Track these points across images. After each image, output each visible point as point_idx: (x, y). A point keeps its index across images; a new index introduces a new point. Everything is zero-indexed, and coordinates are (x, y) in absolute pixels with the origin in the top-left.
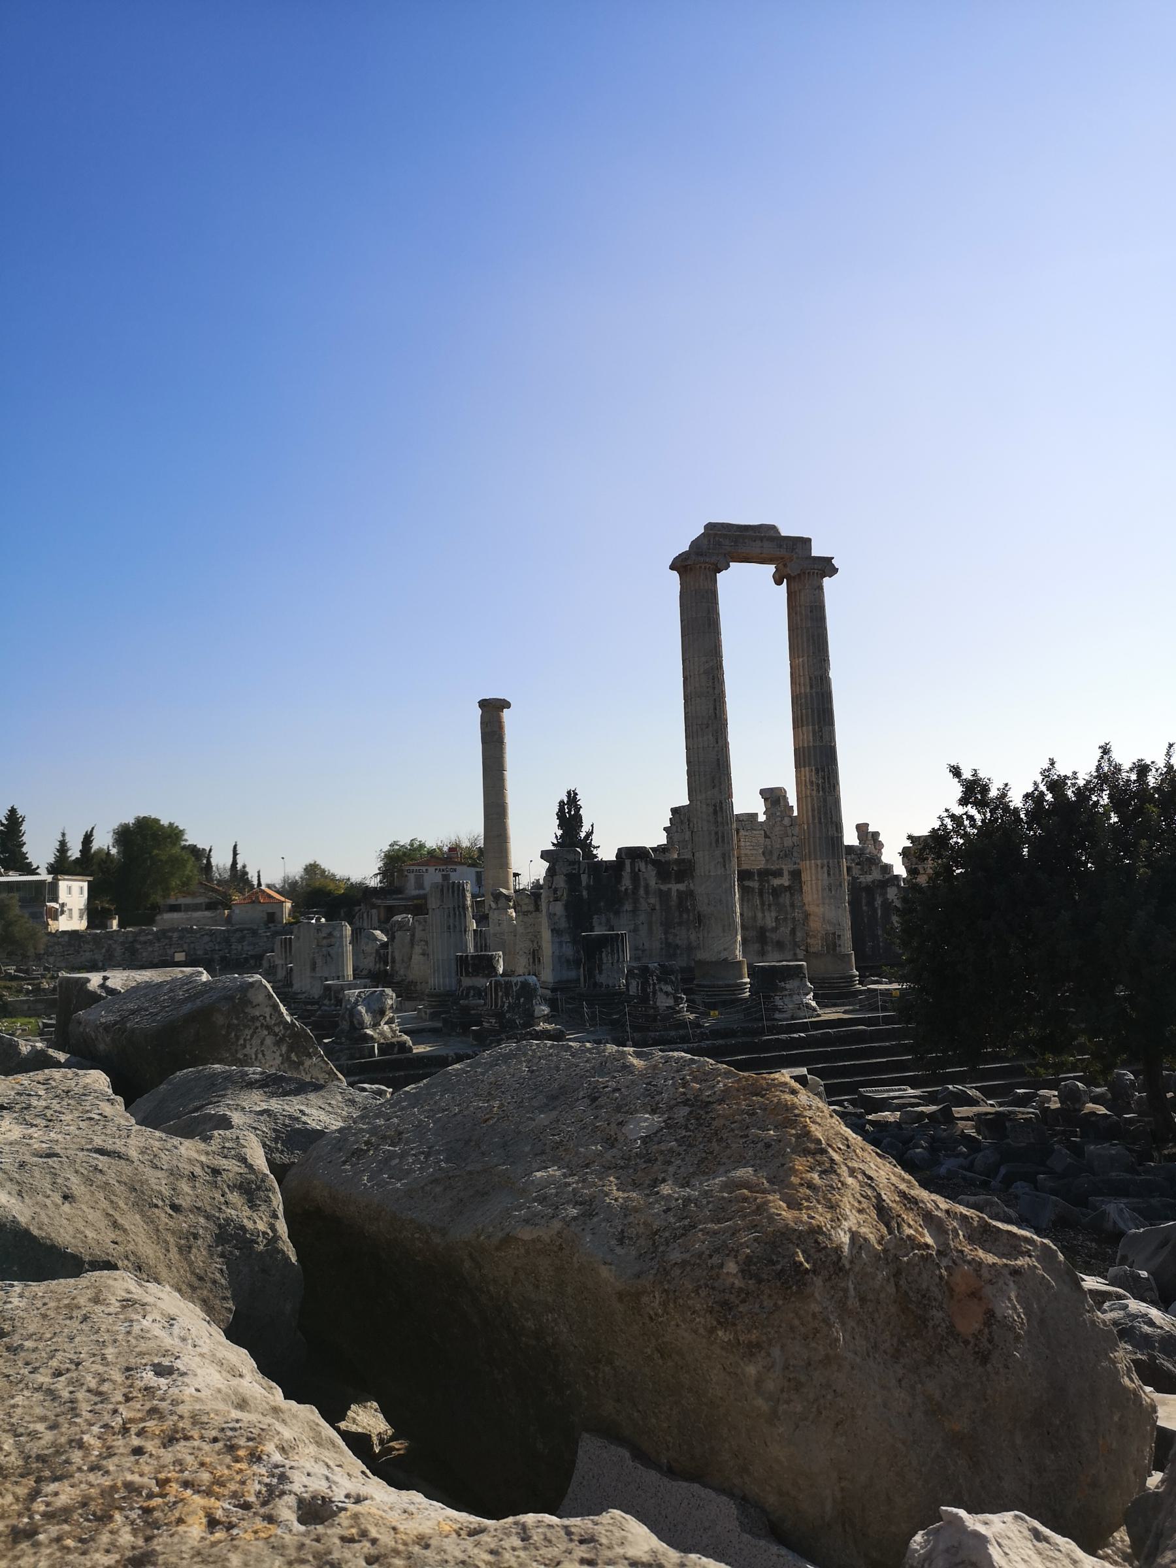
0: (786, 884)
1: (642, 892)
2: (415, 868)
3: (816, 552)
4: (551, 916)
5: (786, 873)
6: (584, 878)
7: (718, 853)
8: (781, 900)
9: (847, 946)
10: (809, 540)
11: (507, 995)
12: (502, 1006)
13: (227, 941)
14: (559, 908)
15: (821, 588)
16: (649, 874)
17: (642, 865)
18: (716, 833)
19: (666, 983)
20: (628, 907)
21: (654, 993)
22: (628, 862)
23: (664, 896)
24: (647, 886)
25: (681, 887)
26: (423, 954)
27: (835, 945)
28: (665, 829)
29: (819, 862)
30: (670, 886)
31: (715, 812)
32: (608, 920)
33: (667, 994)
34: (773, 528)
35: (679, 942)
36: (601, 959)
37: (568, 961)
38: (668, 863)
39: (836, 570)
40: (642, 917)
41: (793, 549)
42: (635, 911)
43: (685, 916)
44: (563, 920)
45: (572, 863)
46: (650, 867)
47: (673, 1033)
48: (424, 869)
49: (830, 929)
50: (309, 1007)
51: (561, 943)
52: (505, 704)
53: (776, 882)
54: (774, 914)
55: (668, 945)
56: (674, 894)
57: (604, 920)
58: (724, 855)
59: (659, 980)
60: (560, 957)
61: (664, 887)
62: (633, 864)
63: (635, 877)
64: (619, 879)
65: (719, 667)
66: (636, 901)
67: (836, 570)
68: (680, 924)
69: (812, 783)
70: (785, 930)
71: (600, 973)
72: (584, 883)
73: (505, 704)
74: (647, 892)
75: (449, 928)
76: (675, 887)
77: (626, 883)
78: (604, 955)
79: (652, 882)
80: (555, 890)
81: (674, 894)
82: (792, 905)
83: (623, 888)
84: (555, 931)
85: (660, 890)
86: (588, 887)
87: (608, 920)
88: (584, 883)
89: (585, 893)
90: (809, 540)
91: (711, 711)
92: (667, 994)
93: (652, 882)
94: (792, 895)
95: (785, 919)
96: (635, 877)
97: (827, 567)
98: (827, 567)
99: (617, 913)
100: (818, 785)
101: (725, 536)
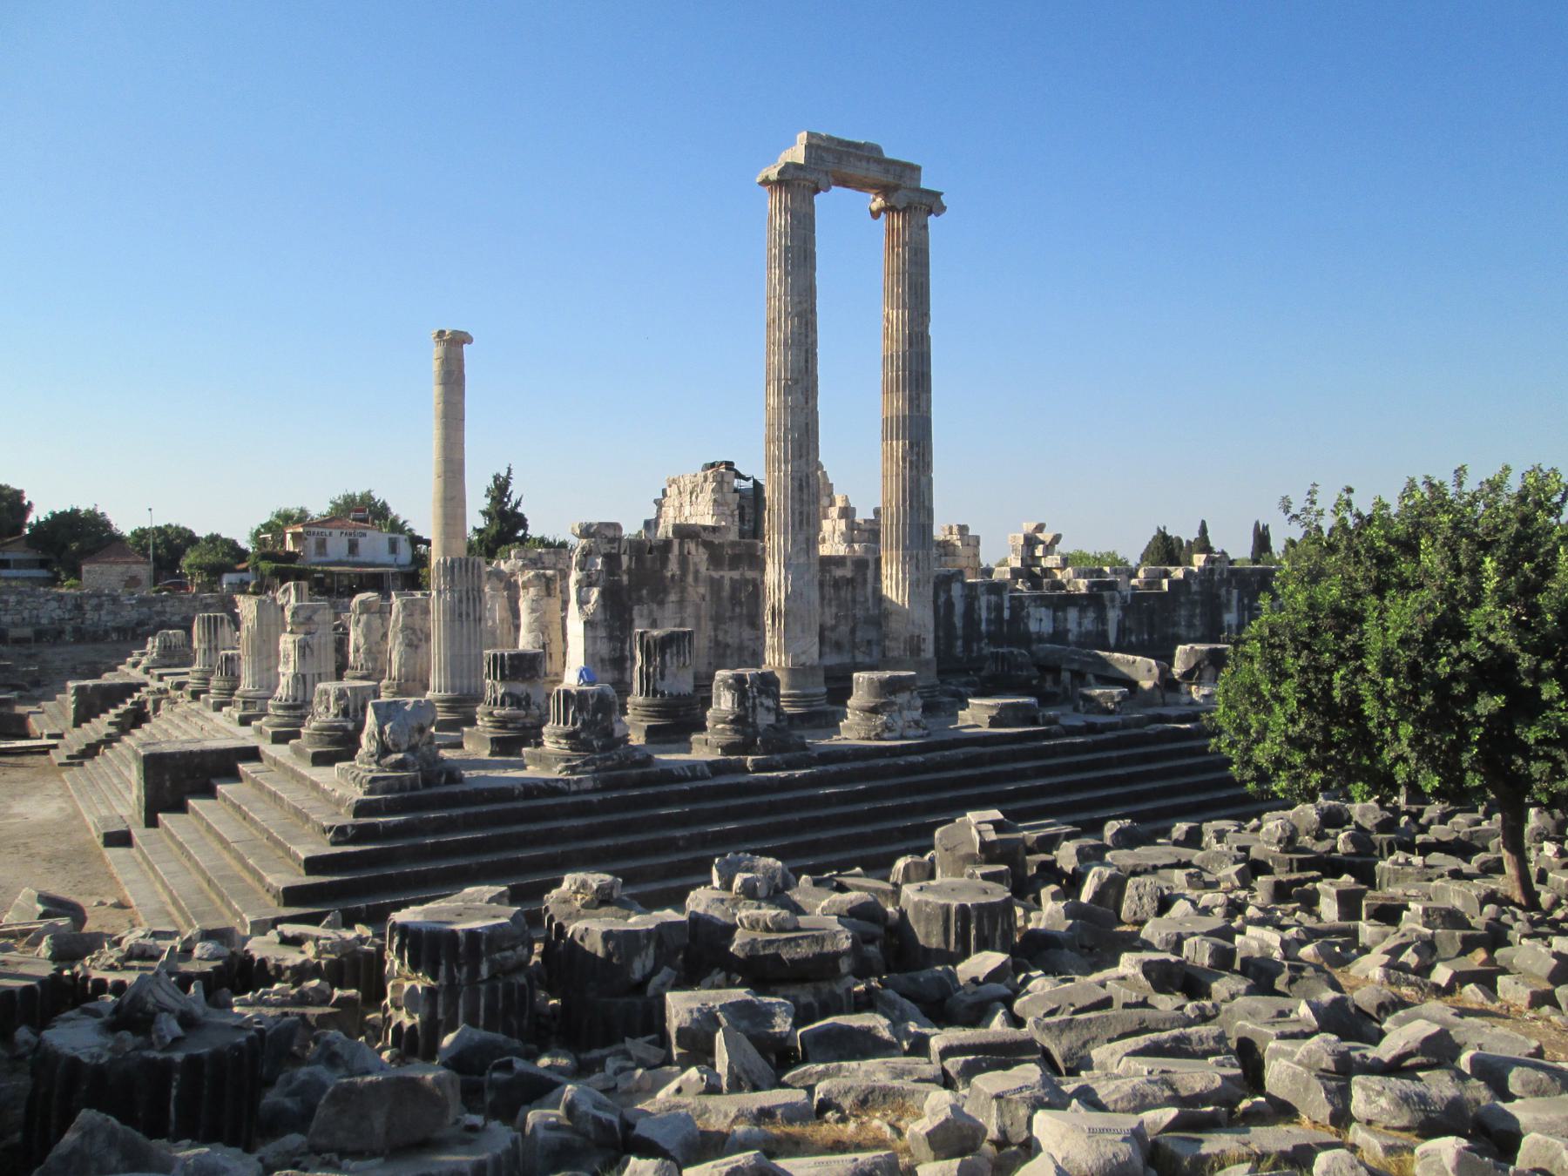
0: (849, 575)
1: (690, 579)
2: (316, 530)
3: (925, 183)
5: (849, 563)
6: (625, 559)
7: (801, 537)
8: (843, 593)
9: (929, 651)
10: (918, 169)
13: (79, 607)
15: (925, 227)
16: (699, 556)
17: (691, 546)
18: (801, 513)
19: (768, 696)
20: (673, 597)
21: (754, 707)
22: (676, 543)
24: (697, 572)
25: (736, 575)
27: (919, 650)
31: (801, 488)
32: (651, 612)
33: (768, 709)
34: (877, 149)
35: (730, 641)
37: (602, 660)
38: (721, 545)
39: (943, 209)
40: (690, 610)
41: (901, 177)
42: (681, 602)
43: (738, 610)
45: (612, 540)
46: (701, 549)
47: (777, 757)
48: (327, 531)
49: (917, 632)
51: (595, 638)
53: (838, 573)
54: (834, 610)
55: (717, 643)
56: (727, 583)
57: (645, 612)
58: (808, 539)
59: (760, 692)
60: (593, 655)
61: (716, 575)
62: (681, 545)
63: (684, 560)
64: (664, 561)
65: (813, 311)
66: (683, 590)
67: (943, 209)
68: (731, 619)
70: (844, 629)
72: (624, 567)
74: (696, 579)
75: (460, 615)
76: (728, 575)
77: (673, 567)
78: (668, 657)
79: (703, 568)
81: (727, 583)
82: (854, 601)
83: (669, 574)
84: (588, 624)
85: (712, 579)
86: (629, 570)
87: (651, 612)
88: (624, 567)
89: (625, 578)
90: (918, 169)
91: (803, 364)
92: (768, 709)
93: (703, 568)
94: (854, 588)
95: (846, 617)
96: (684, 560)
97: (931, 203)
98: (931, 203)
99: (661, 603)
101: (827, 150)
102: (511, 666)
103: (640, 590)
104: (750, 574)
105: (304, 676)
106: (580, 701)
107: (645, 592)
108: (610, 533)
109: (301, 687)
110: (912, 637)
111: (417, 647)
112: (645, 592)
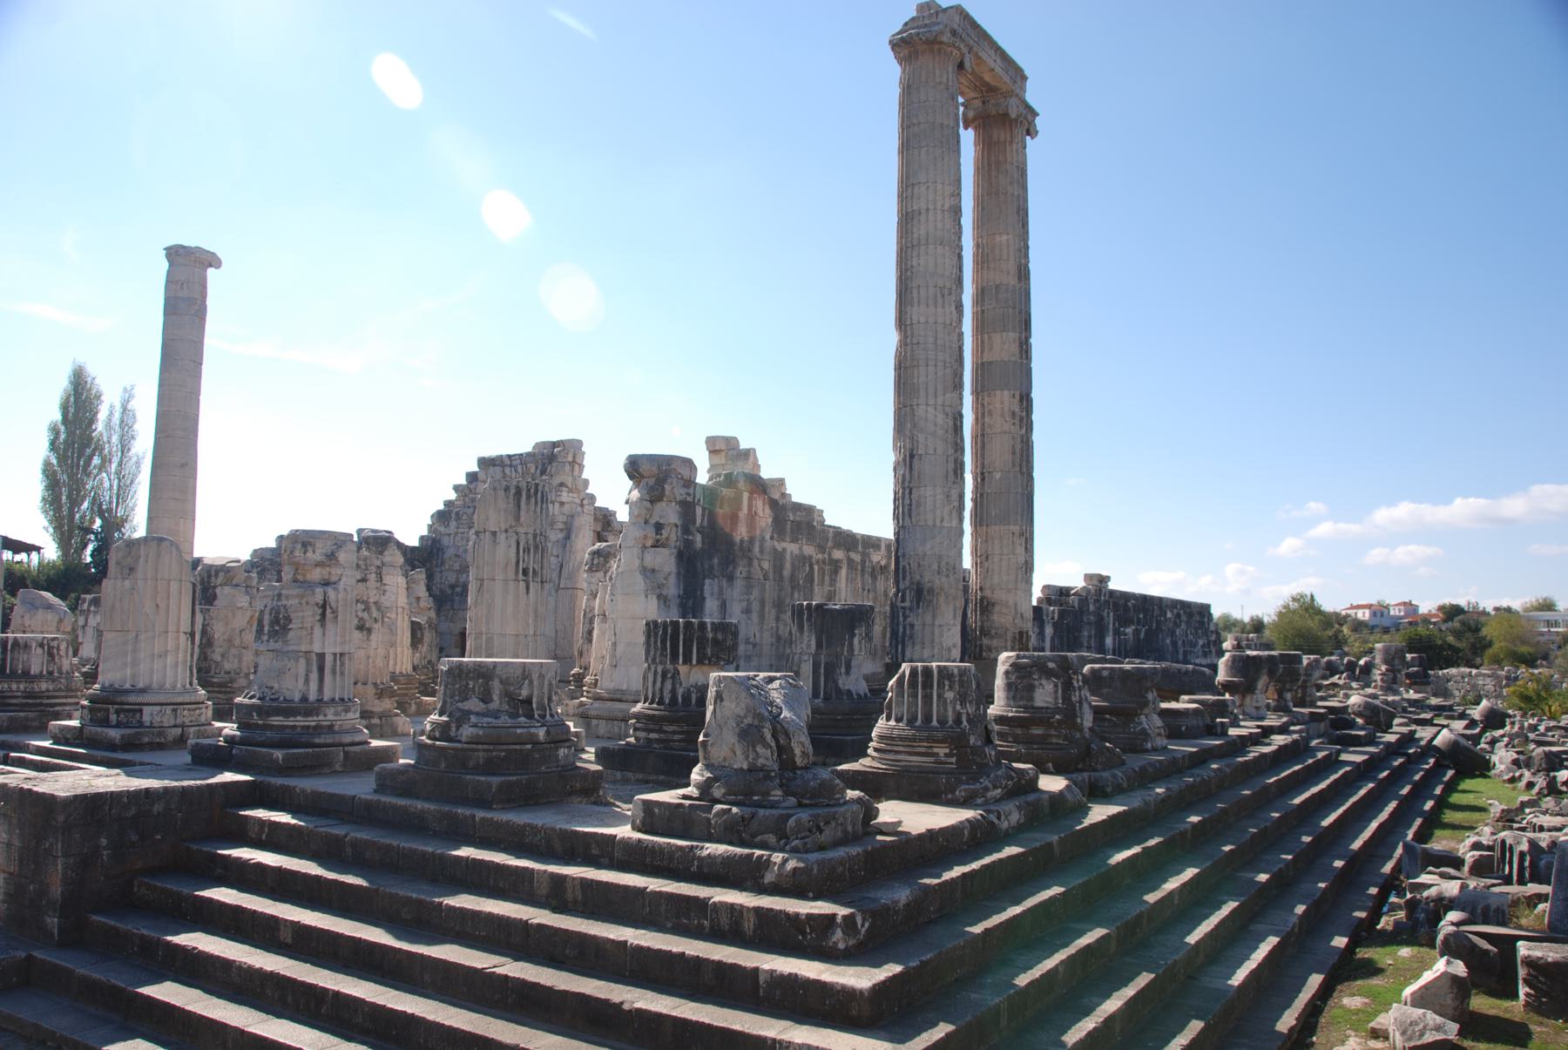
4: (648, 572)
11: (962, 698)
12: (958, 721)
14: (665, 560)
21: (1081, 703)
23: (778, 557)
26: (360, 628)
28: (457, 488)
29: (1016, 529)
30: (784, 545)
36: (851, 645)
44: (672, 580)
50: (277, 720)
52: (212, 261)
56: (788, 557)
57: (716, 589)
61: (779, 546)
62: (750, 500)
69: (1013, 414)
71: (848, 673)
73: (212, 261)
74: (761, 552)
75: (525, 572)
76: (792, 548)
80: (659, 527)
85: (775, 550)
89: (699, 538)
100: (1021, 419)
102: (715, 641)
103: (711, 558)
104: (809, 550)
105: (321, 657)
106: (961, 683)
107: (716, 561)
108: (685, 473)
109: (314, 676)
110: (1021, 633)
111: (369, 631)
112: (716, 561)
